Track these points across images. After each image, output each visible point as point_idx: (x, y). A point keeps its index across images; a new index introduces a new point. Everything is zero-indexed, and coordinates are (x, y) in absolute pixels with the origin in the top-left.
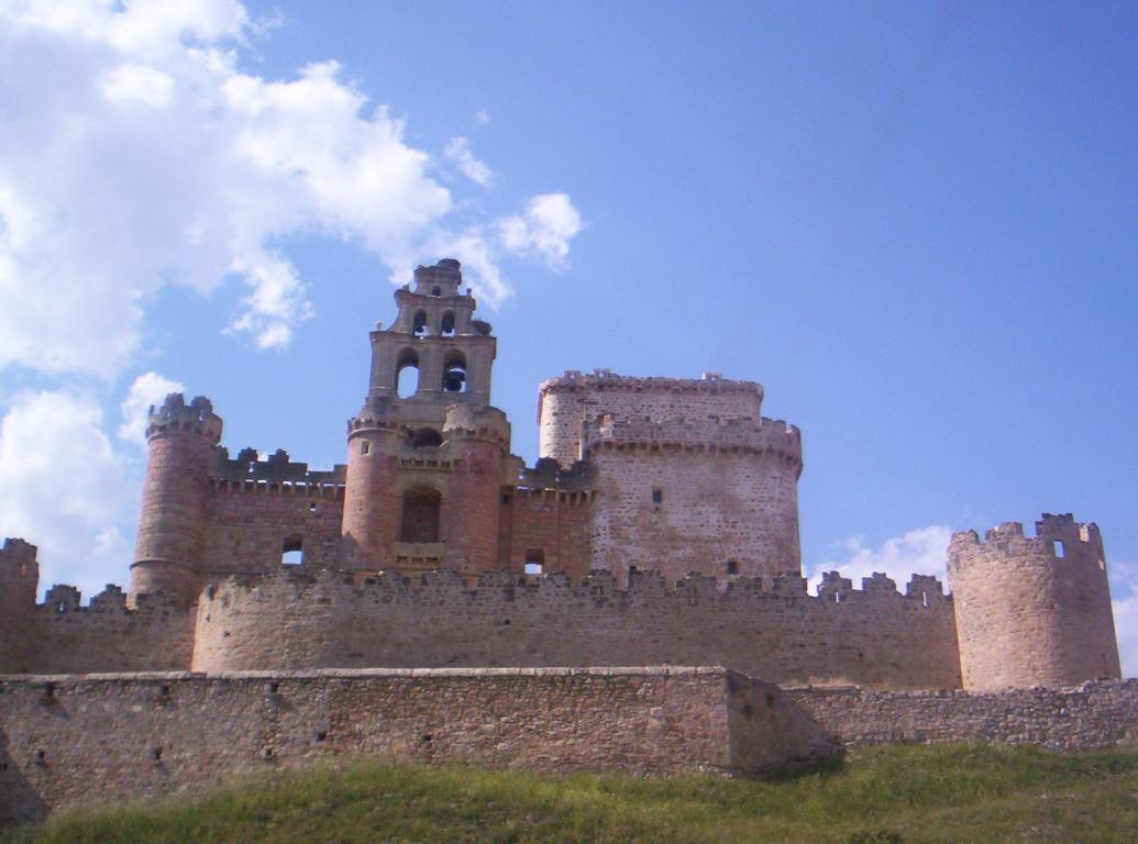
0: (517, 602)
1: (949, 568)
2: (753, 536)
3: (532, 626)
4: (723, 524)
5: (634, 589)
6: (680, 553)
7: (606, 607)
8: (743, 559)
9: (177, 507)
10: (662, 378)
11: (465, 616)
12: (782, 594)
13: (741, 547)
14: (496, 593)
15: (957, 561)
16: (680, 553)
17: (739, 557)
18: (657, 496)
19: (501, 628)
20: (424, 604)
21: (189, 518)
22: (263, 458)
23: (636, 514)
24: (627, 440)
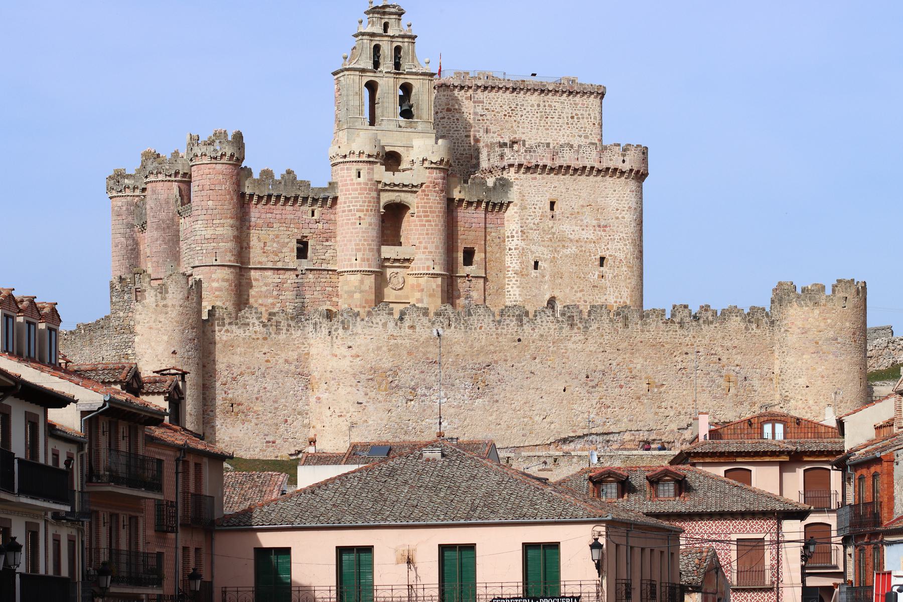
0: (525, 327)
1: (773, 302)
2: (617, 237)
5: (592, 317)
6: (568, 252)
7: (576, 330)
8: (610, 256)
11: (494, 336)
12: (677, 320)
13: (609, 246)
14: (512, 321)
15: (781, 300)
16: (568, 252)
17: (606, 254)
20: (471, 329)
22: (277, 177)
24: (534, 162)
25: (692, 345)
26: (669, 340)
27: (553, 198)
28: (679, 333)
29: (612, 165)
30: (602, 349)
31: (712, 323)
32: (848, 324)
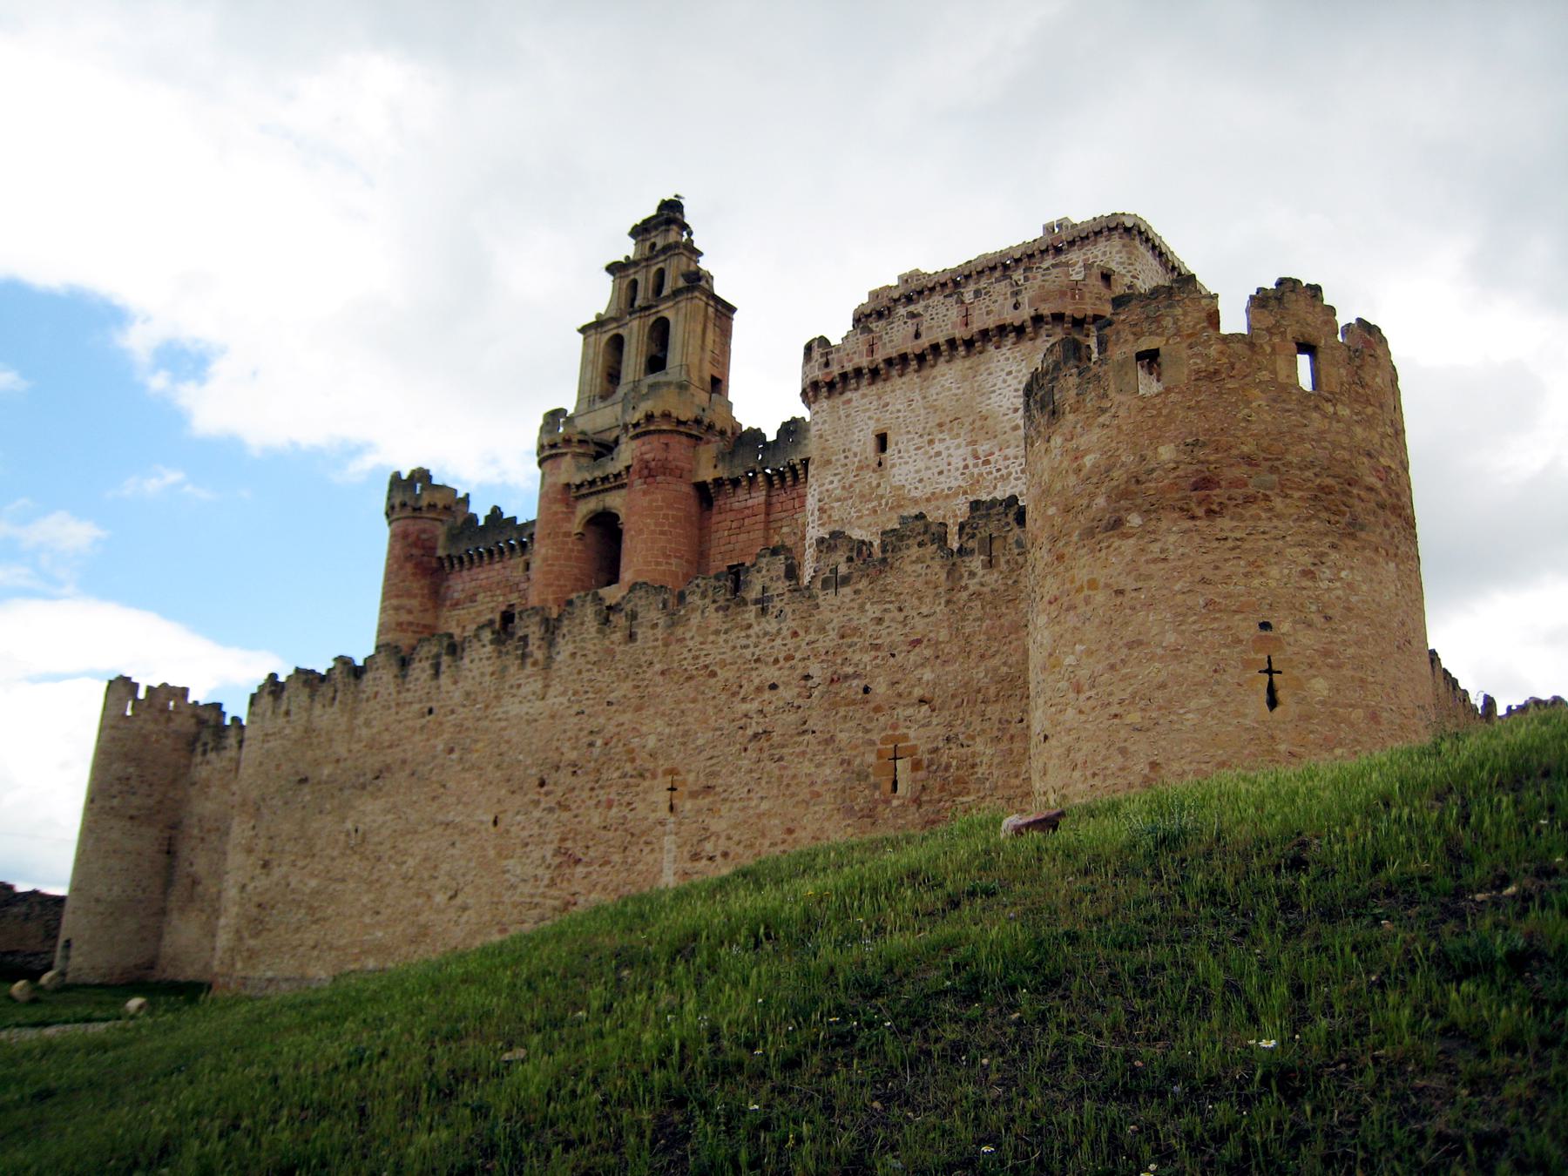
3: (453, 712)
4: (971, 462)
7: (529, 669)
9: (395, 602)
10: (985, 256)
18: (882, 441)
19: (424, 721)
21: (410, 612)
25: (789, 658)
26: (728, 657)
27: (881, 427)
28: (756, 628)
29: (991, 323)
30: (576, 708)
31: (846, 580)
32: (1166, 453)
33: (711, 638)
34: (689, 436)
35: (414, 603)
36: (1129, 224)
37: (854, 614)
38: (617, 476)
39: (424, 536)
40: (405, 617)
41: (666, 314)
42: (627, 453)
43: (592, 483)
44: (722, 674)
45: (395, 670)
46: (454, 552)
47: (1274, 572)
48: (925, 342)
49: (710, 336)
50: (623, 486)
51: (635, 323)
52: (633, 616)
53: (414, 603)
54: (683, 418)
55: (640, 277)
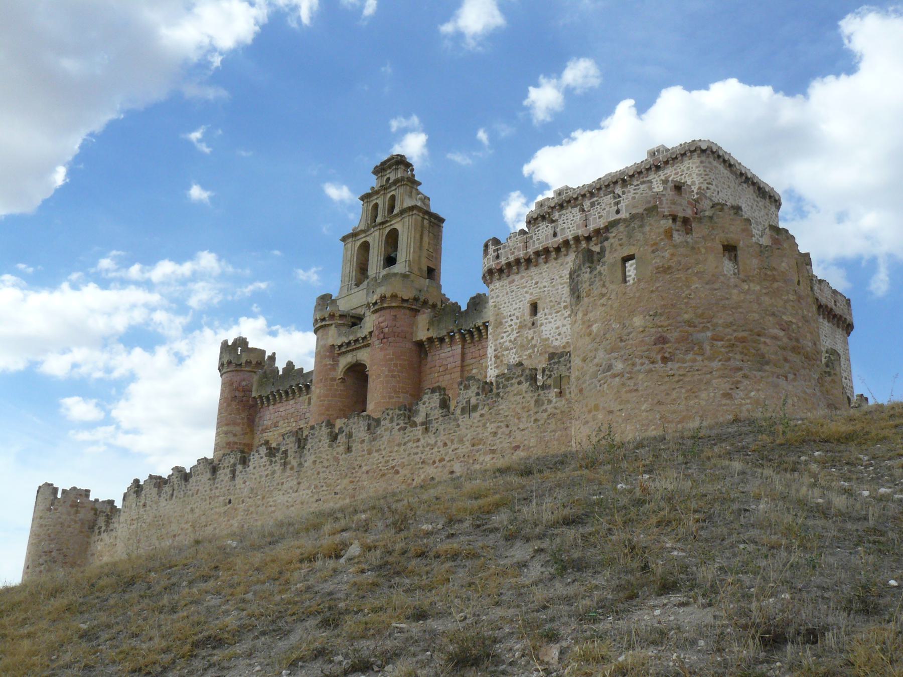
3: (243, 502)
7: (288, 472)
9: (225, 429)
10: (610, 174)
19: (226, 508)
21: (235, 435)
23: (516, 335)
25: (442, 460)
27: (533, 298)
28: (422, 441)
30: (316, 497)
31: (475, 408)
33: (396, 448)
34: (411, 309)
35: (238, 429)
36: (704, 147)
37: (480, 430)
38: (364, 338)
39: (244, 383)
40: (232, 439)
41: (397, 226)
42: (370, 322)
43: (349, 344)
44: (403, 472)
45: (209, 475)
46: (264, 394)
47: (704, 395)
48: (560, 239)
49: (426, 239)
50: (368, 345)
51: (377, 233)
52: (350, 436)
53: (238, 429)
54: (405, 298)
55: (380, 202)
